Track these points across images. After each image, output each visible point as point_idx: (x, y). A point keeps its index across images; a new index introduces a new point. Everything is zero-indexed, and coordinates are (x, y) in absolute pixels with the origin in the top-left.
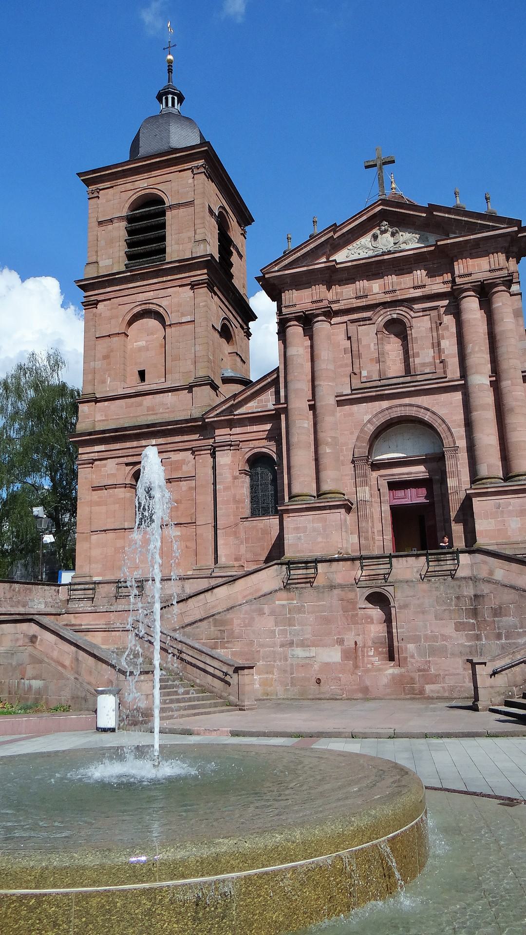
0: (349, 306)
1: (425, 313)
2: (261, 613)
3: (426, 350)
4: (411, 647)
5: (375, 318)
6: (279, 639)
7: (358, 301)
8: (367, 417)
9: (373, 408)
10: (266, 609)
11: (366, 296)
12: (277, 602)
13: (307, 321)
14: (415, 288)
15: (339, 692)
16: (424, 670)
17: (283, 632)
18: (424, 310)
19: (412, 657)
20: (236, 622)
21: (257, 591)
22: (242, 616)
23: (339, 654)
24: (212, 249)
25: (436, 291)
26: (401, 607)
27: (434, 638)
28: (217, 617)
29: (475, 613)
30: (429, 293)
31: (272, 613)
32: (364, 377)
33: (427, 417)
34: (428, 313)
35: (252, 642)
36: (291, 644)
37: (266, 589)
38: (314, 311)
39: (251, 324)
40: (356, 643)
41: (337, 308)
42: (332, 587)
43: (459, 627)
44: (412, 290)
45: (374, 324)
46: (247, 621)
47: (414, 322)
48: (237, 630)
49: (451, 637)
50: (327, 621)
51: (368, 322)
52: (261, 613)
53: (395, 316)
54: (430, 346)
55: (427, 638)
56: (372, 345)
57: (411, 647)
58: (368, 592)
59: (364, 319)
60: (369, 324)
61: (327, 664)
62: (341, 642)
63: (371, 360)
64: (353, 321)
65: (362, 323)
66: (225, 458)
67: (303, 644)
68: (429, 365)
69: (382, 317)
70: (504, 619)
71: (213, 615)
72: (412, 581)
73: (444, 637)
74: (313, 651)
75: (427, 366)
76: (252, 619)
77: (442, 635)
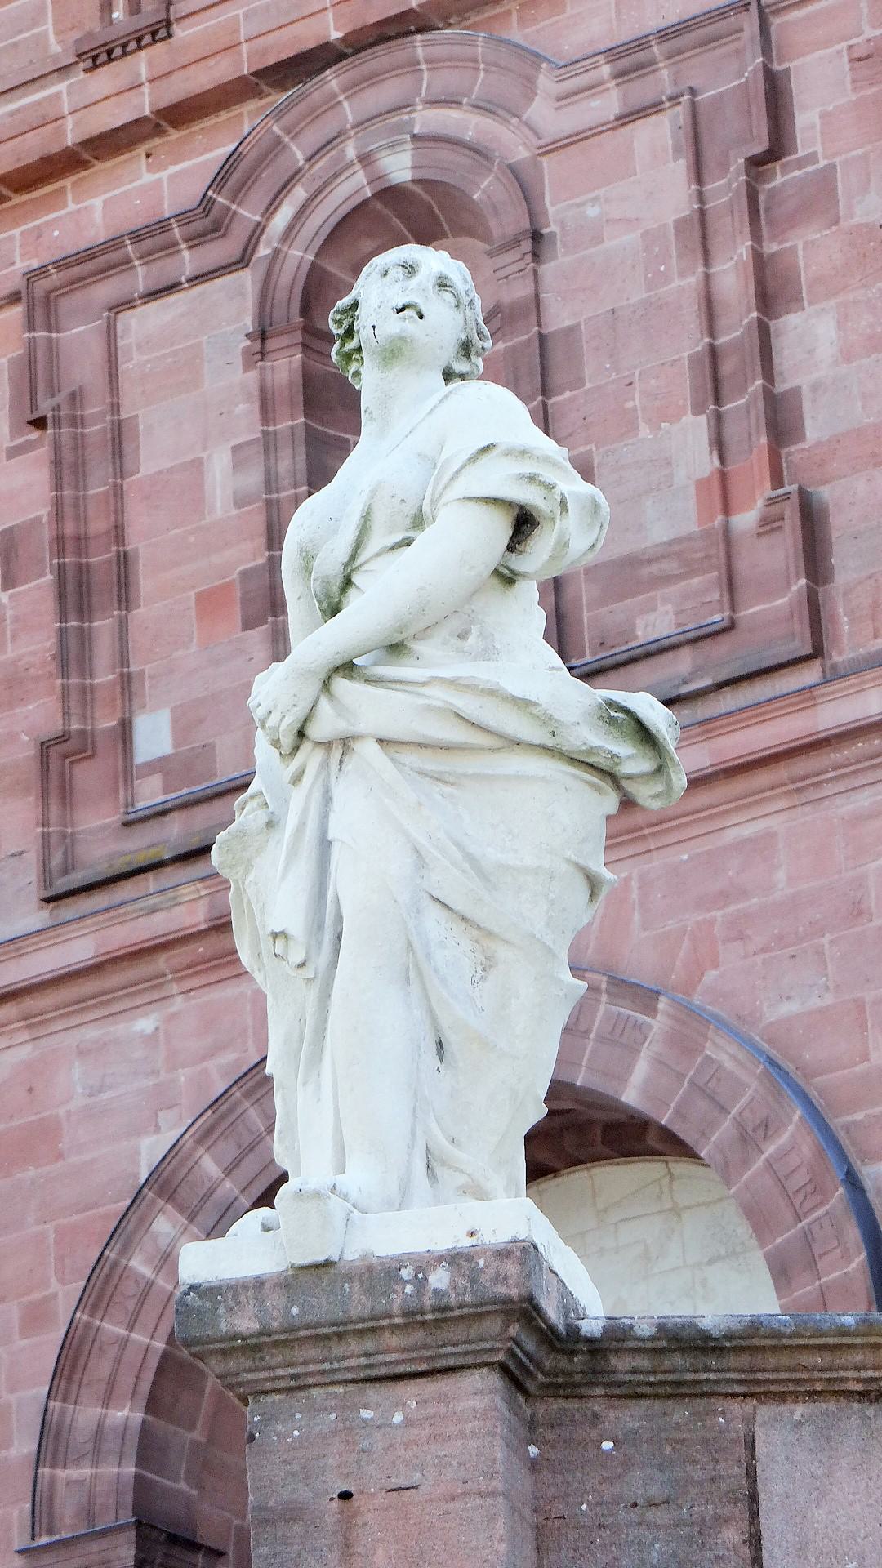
1: (643, 91)
3: (645, 431)
5: (249, 214)
7: (105, 80)
8: (151, 1149)
9: (211, 1054)
32: (158, 765)
33: (641, 1069)
45: (243, 261)
51: (188, 261)
53: (399, 167)
54: (682, 386)
56: (219, 464)
60: (198, 279)
63: (209, 602)
65: (141, 277)
68: (670, 566)
69: (299, 194)
75: (668, 579)
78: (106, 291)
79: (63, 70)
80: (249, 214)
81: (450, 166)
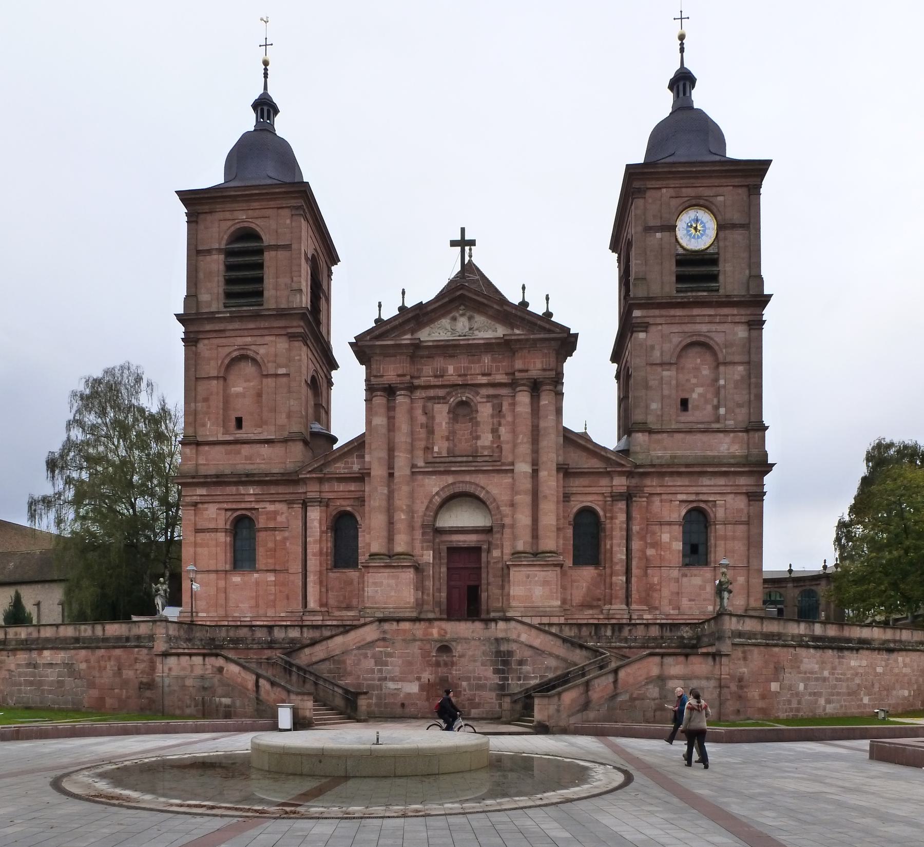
0: (428, 384)
2: (366, 656)
4: (464, 684)
6: (377, 676)
7: (436, 380)
10: (369, 653)
11: (442, 376)
12: (377, 649)
13: (390, 391)
14: (484, 375)
15: (416, 713)
16: (472, 700)
17: (380, 671)
18: (488, 396)
19: (465, 690)
20: (348, 662)
21: (364, 640)
22: (353, 658)
23: (418, 688)
24: (304, 300)
25: (499, 381)
26: (460, 657)
27: (480, 679)
28: (335, 658)
29: (506, 663)
30: (493, 381)
31: (373, 657)
34: (490, 399)
35: (359, 677)
36: (385, 679)
37: (369, 639)
38: (398, 385)
39: (334, 373)
40: (429, 680)
41: (417, 384)
42: (415, 640)
43: (497, 671)
44: (480, 377)
46: (356, 662)
47: (481, 408)
48: (349, 669)
49: (490, 678)
50: (410, 664)
51: (442, 401)
52: (366, 656)
53: (464, 399)
55: (475, 678)
57: (464, 684)
58: (438, 645)
59: (439, 398)
61: (409, 694)
62: (419, 679)
64: (430, 399)
65: (437, 401)
66: (315, 515)
67: (393, 679)
70: (524, 667)
71: (332, 657)
72: (469, 639)
73: (486, 679)
74: (399, 685)
76: (360, 660)
77: (485, 677)
78: (433, 401)
79: (432, 377)
80: (448, 398)
81: (468, 400)
